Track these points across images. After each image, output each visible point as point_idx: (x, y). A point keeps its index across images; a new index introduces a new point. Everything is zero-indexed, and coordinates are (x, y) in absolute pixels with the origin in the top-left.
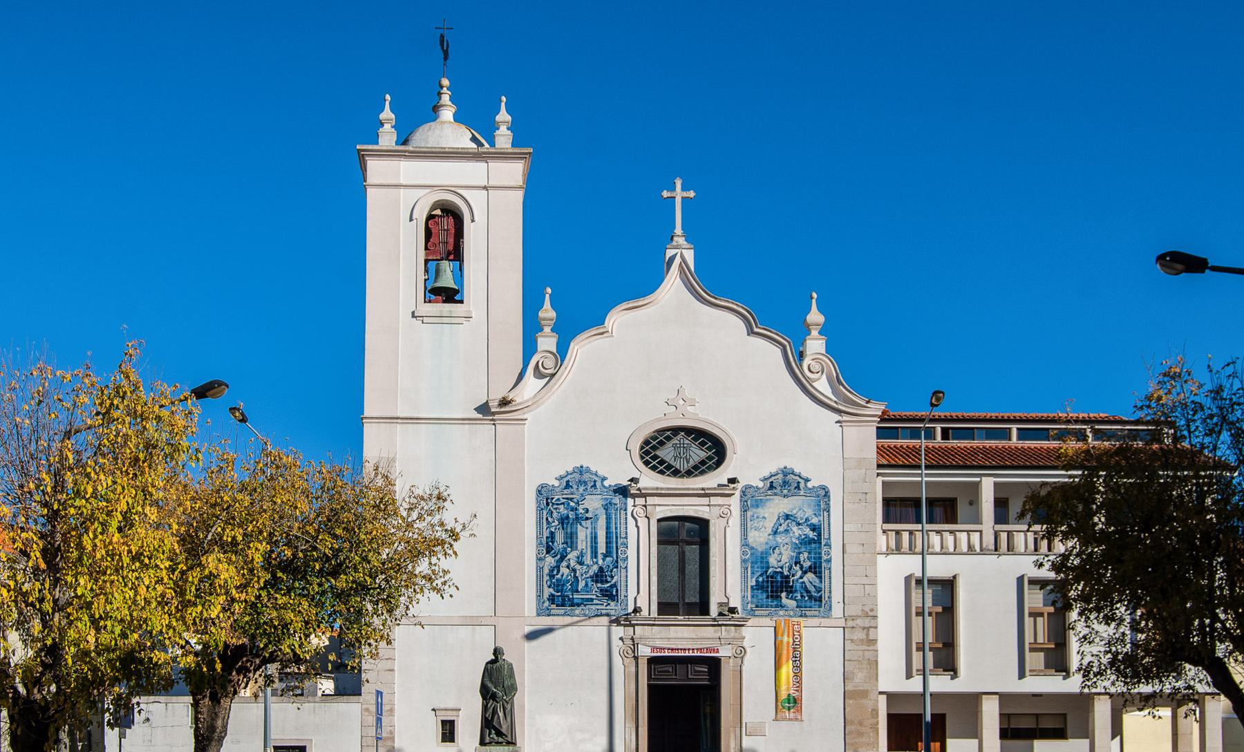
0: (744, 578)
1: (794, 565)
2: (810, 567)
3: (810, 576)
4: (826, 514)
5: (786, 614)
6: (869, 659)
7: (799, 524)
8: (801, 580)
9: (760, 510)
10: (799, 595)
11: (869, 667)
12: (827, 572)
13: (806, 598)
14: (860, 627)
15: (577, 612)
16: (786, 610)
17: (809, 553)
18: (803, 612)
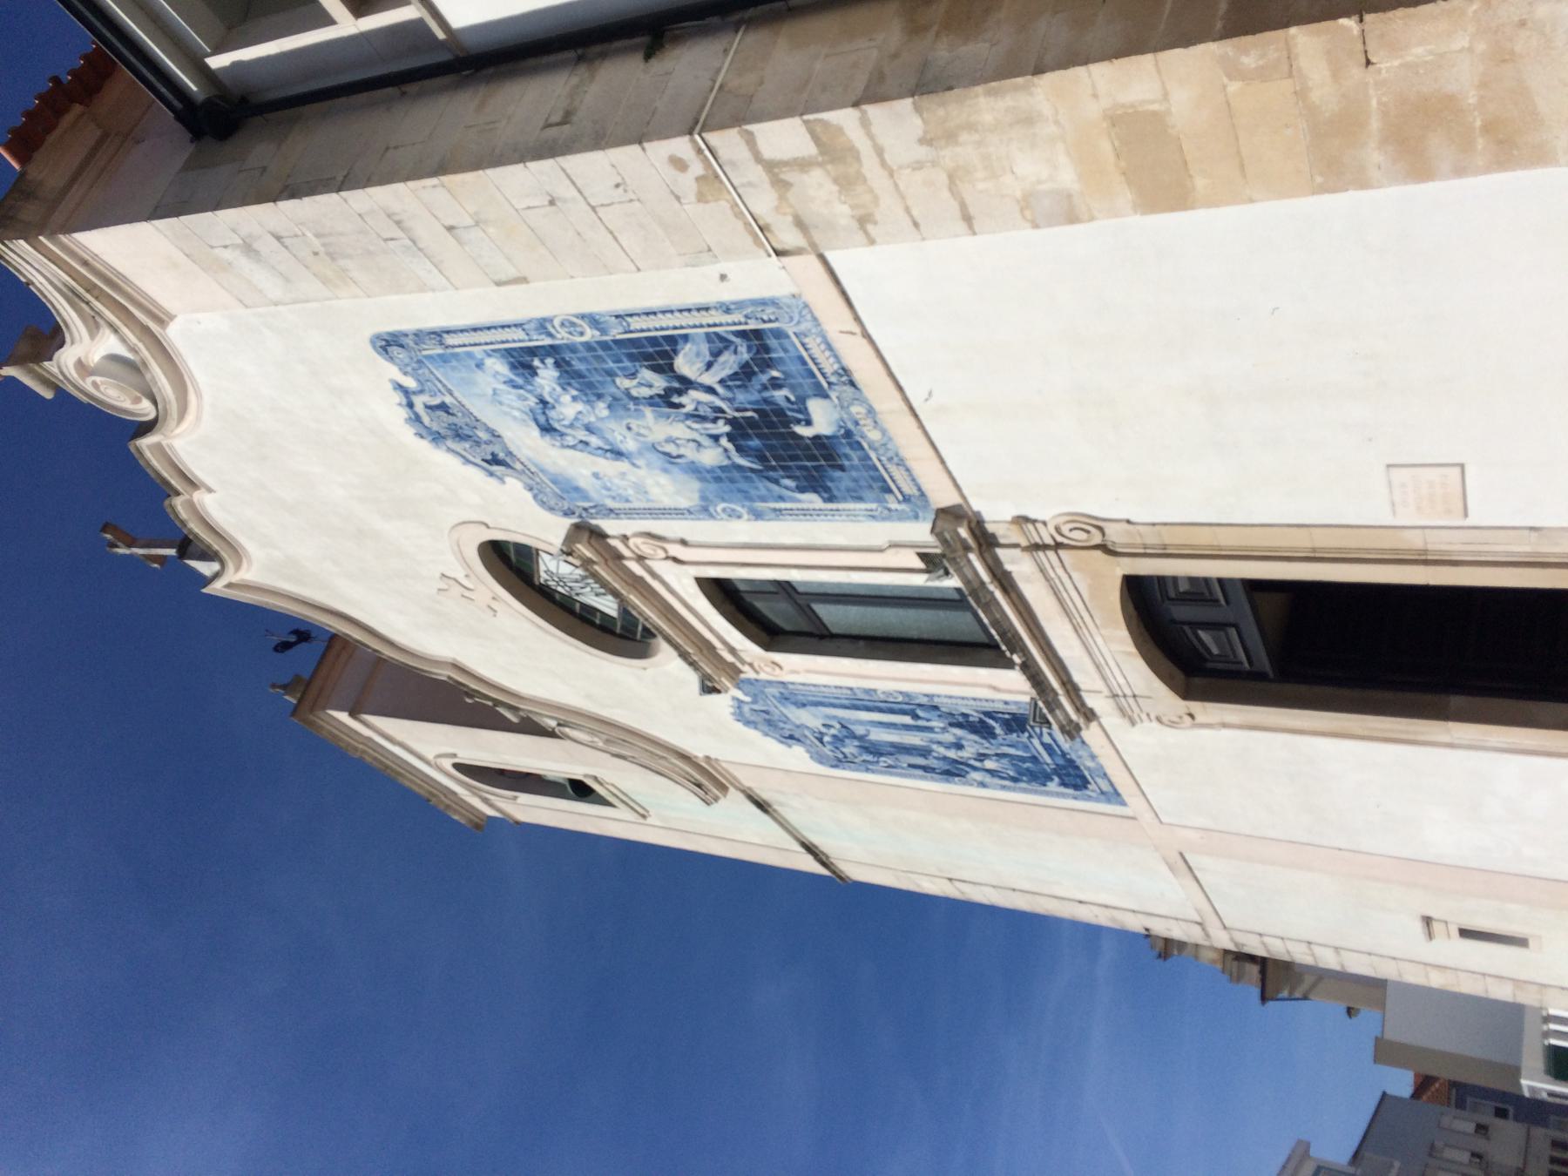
0: (806, 513)
1: (684, 410)
2: (657, 369)
3: (685, 364)
4: (450, 340)
5: (869, 421)
6: (923, 141)
7: (543, 402)
8: (720, 389)
9: (582, 484)
10: (779, 395)
11: (964, 137)
12: (636, 323)
13: (775, 373)
14: (782, 198)
15: (1090, 764)
16: (857, 423)
17: (611, 374)
18: (833, 379)
